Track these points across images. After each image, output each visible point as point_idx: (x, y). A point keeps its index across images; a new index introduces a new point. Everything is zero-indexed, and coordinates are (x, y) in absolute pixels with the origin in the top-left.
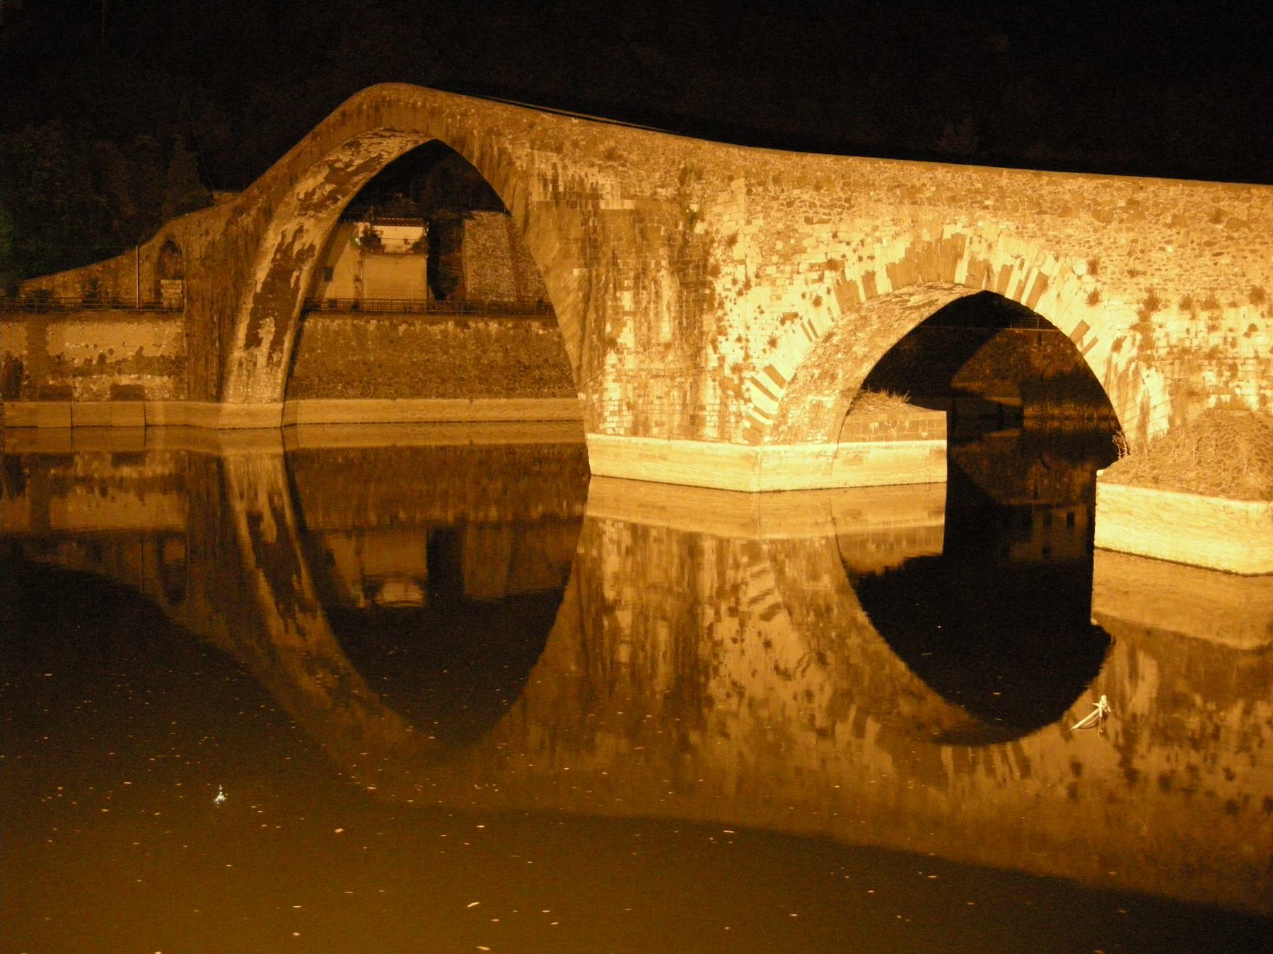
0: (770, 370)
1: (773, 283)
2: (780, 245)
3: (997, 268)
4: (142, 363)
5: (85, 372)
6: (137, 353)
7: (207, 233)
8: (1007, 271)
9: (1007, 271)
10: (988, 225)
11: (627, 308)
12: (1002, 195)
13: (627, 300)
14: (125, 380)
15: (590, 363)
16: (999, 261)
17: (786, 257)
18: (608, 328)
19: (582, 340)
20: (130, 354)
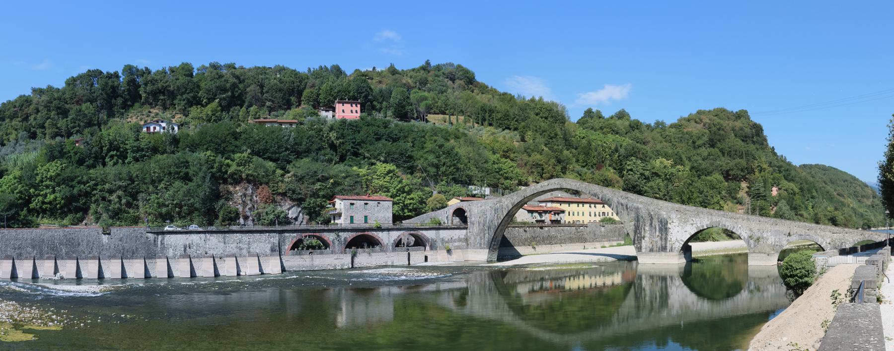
0: (682, 240)
1: (682, 226)
2: (683, 220)
3: (726, 226)
4: (460, 240)
5: (447, 242)
6: (459, 237)
7: (481, 207)
8: (728, 226)
9: (728, 226)
10: (724, 219)
11: (647, 229)
12: (727, 215)
13: (647, 228)
14: (456, 244)
15: (637, 240)
16: (727, 224)
17: (685, 222)
18: (642, 233)
19: (635, 235)
20: (457, 237)
